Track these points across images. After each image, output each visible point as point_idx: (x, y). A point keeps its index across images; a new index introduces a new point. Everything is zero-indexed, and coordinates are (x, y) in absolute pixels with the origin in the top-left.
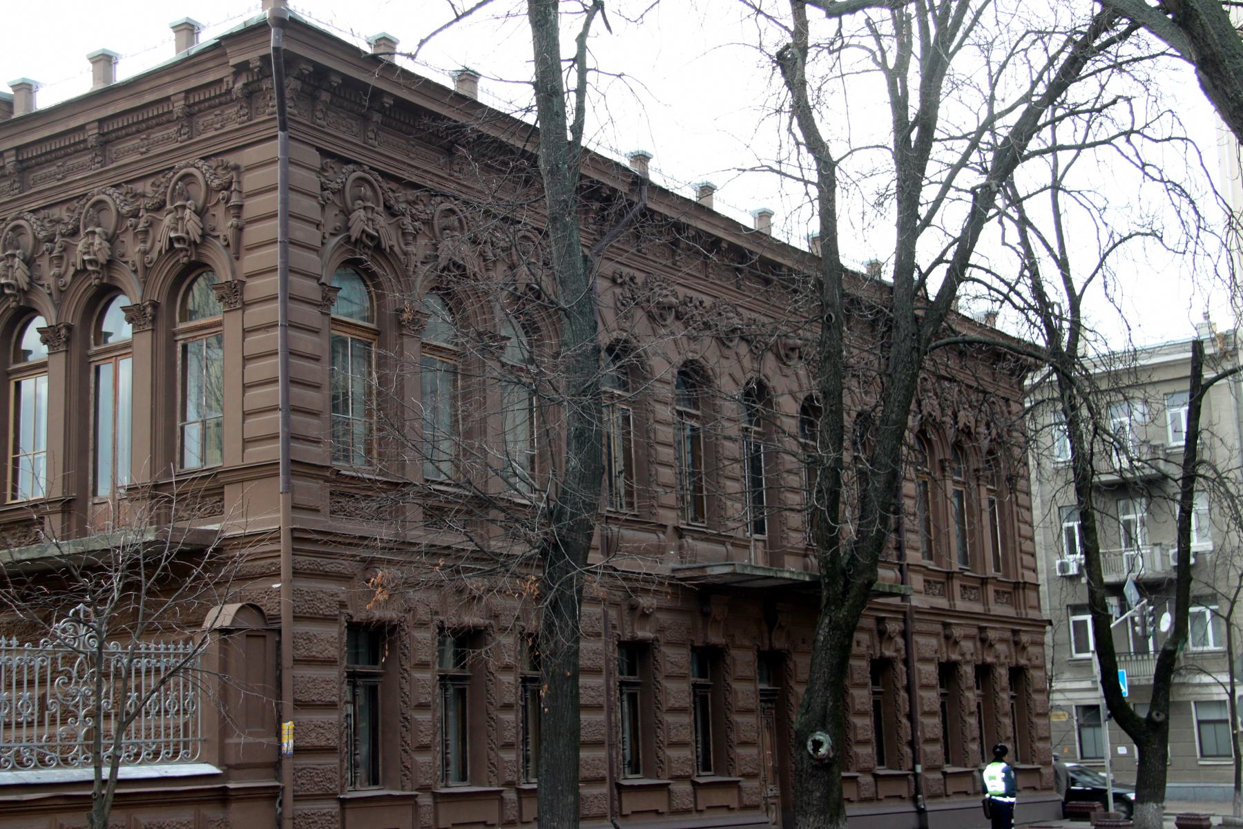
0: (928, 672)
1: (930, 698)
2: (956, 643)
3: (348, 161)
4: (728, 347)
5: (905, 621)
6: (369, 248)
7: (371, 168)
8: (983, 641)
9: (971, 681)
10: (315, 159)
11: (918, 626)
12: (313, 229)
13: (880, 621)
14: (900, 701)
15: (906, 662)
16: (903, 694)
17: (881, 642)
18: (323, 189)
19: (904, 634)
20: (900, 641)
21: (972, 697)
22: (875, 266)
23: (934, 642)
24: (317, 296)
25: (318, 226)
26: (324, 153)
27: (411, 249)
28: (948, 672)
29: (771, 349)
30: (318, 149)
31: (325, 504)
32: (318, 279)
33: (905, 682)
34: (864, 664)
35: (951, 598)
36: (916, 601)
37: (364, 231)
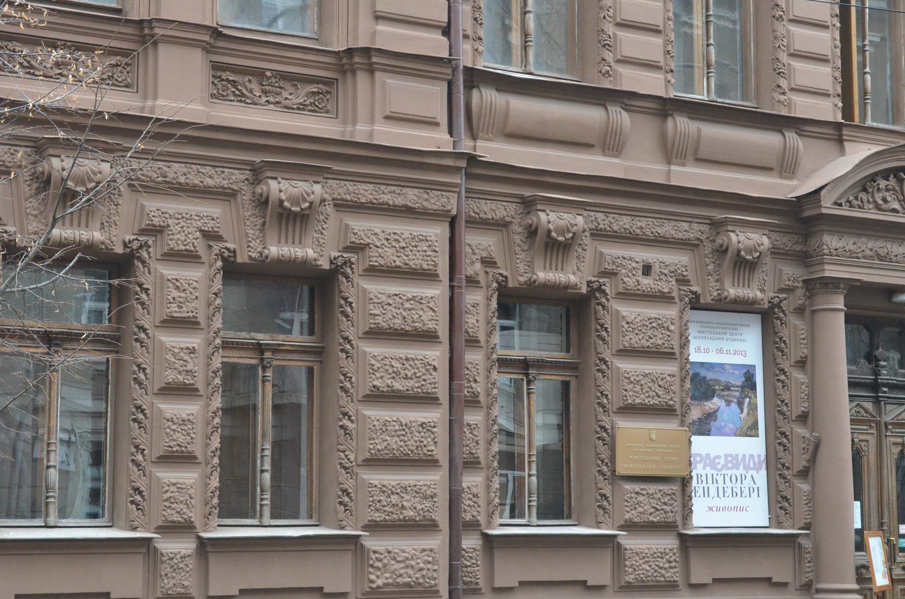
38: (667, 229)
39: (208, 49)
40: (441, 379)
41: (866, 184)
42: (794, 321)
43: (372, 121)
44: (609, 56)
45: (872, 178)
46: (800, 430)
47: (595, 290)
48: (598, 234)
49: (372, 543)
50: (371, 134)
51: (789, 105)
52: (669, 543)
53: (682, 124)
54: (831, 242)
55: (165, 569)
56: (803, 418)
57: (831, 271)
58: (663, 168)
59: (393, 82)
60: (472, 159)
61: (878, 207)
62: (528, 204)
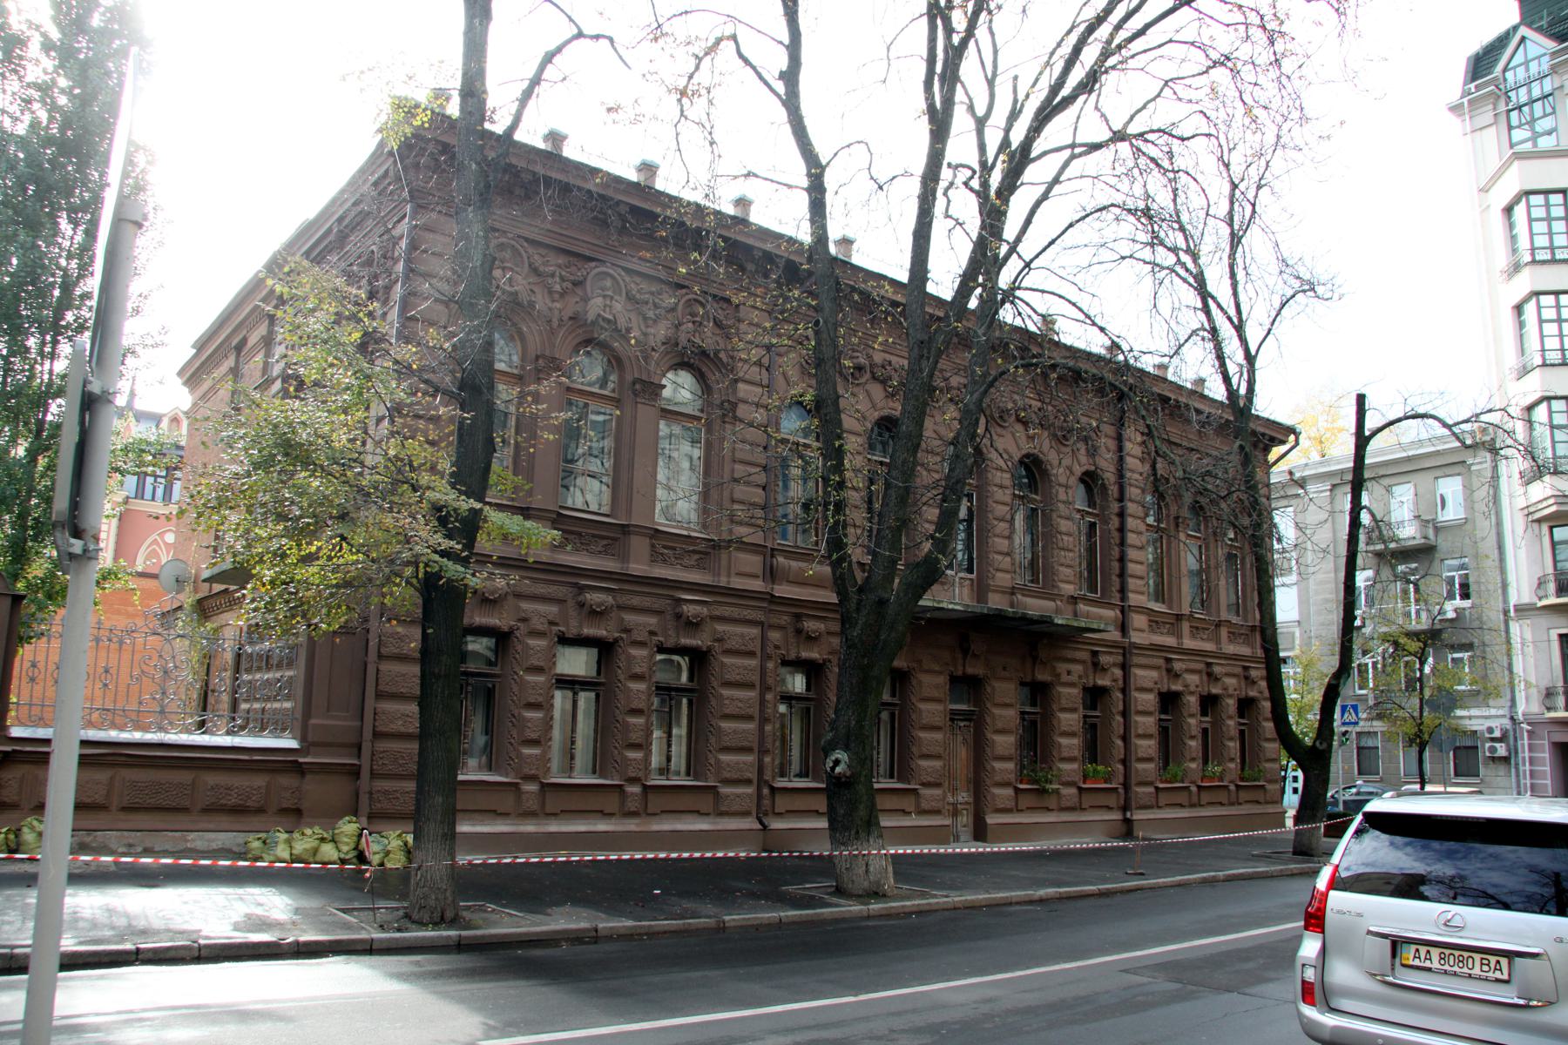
0: (1148, 700)
1: (1146, 724)
3: (591, 259)
5: (1124, 655)
8: (1209, 675)
11: (1136, 660)
13: (1095, 654)
14: (1114, 724)
15: (1124, 691)
16: (1119, 718)
17: (1095, 672)
19: (1124, 667)
20: (1118, 672)
21: (1193, 723)
22: (440, 94)
23: (1154, 674)
27: (652, 331)
28: (1169, 701)
33: (1121, 707)
34: (1075, 692)
35: (1180, 636)
36: (1136, 638)
37: (599, 315)
39: (651, 537)
43: (729, 575)
50: (729, 582)
52: (1152, 790)
59: (742, 556)
62: (798, 617)
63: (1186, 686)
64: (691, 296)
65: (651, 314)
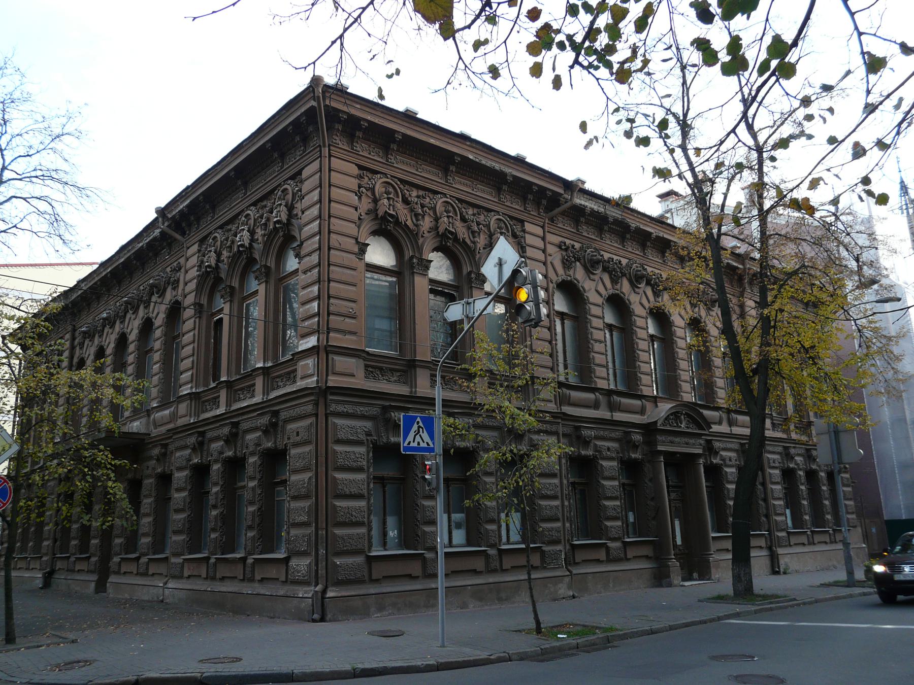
1: (777, 488)
2: (792, 458)
4: (639, 288)
6: (450, 239)
7: (392, 176)
9: (803, 480)
10: (355, 170)
12: (353, 210)
18: (359, 187)
24: (356, 249)
25: (356, 210)
26: (360, 167)
28: (788, 475)
29: (579, 260)
30: (356, 165)
31: (361, 373)
32: (357, 239)
38: (613, 435)
40: (559, 489)
41: (667, 418)
42: (648, 465)
44: (593, 376)
45: (668, 416)
46: (652, 503)
47: (595, 457)
48: (597, 438)
49: (546, 548)
51: (641, 390)
53: (616, 398)
54: (659, 438)
55: (491, 560)
56: (652, 499)
57: (660, 448)
58: (609, 414)
60: (564, 414)
61: (670, 425)
63: (797, 464)
64: (445, 199)
65: (476, 229)
